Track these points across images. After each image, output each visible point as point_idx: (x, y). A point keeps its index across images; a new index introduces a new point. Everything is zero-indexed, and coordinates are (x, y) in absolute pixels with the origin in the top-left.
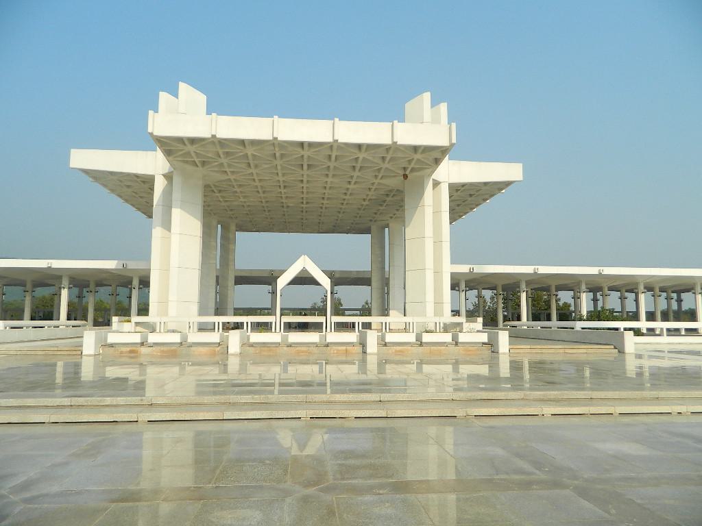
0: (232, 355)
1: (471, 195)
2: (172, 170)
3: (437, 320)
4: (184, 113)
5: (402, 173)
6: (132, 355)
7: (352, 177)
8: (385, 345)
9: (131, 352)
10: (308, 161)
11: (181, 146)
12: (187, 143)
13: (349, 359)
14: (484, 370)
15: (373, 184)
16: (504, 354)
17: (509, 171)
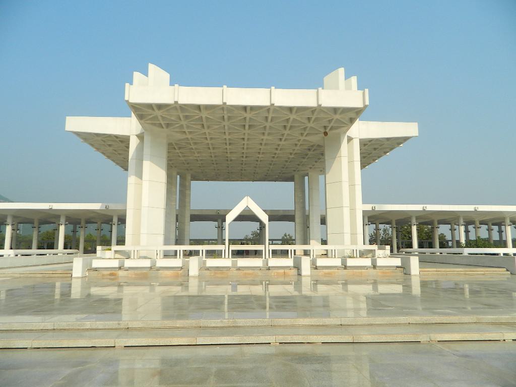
0: (193, 277)
1: (375, 149)
2: (143, 131)
3: (354, 247)
4: (153, 86)
5: (323, 130)
6: (113, 277)
7: (283, 135)
8: (316, 268)
9: (111, 274)
10: (250, 122)
11: (150, 111)
12: (155, 108)
13: (287, 279)
14: (398, 289)
16: (415, 275)
17: (409, 129)
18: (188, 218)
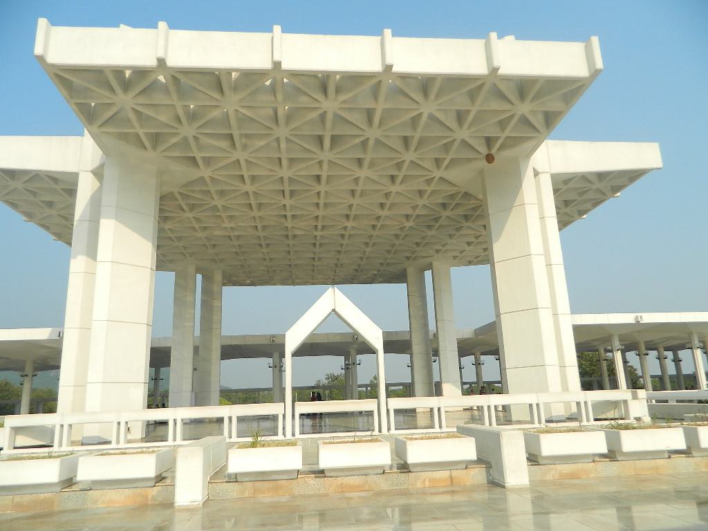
3: (568, 397)
7: (399, 166)
15: (429, 182)
17: (640, 155)
18: (216, 353)
